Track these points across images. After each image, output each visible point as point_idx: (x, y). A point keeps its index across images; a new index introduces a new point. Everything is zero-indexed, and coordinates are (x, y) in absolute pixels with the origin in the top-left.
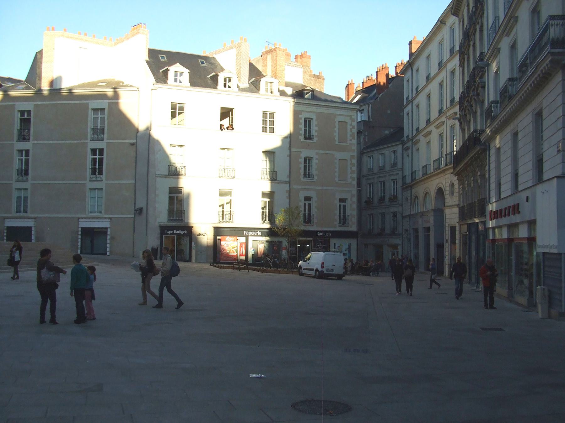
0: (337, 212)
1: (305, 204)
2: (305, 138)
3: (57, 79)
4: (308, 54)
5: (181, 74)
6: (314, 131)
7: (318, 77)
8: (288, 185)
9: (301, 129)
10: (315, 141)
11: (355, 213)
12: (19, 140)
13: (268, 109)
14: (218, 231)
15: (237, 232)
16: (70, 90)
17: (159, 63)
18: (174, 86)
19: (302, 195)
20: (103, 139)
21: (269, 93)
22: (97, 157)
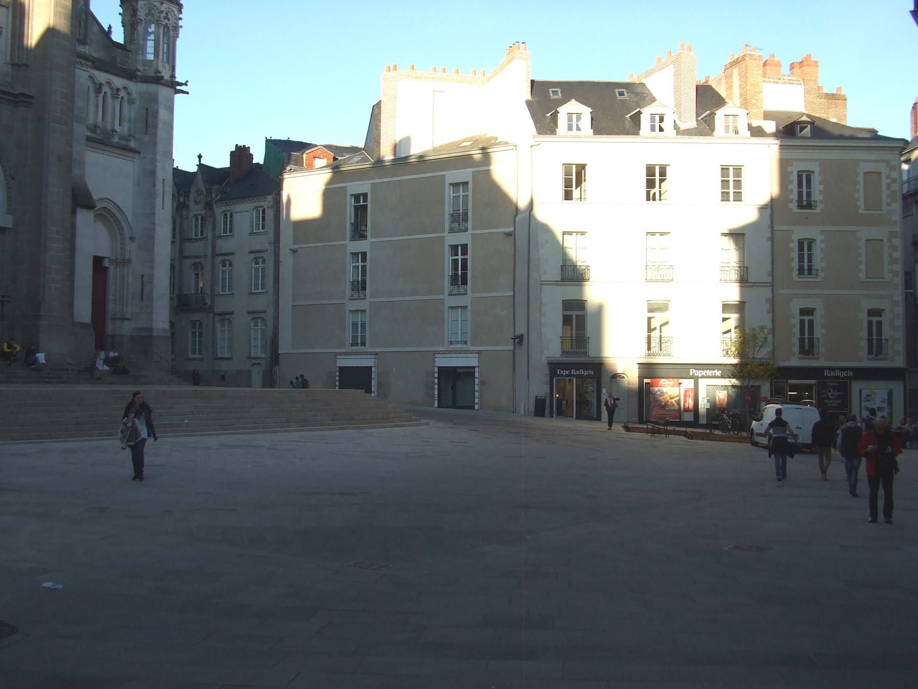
0: (864, 334)
1: (802, 322)
2: (801, 206)
3: (401, 141)
4: (813, 59)
5: (579, 116)
6: (817, 193)
7: (836, 98)
8: (769, 290)
9: (791, 191)
10: (818, 210)
11: (900, 334)
12: (353, 239)
13: (657, 160)
14: (649, 370)
15: (681, 371)
16: (421, 157)
17: (545, 101)
18: (567, 137)
19: (796, 305)
20: (466, 230)
21: (731, 134)
22: (460, 257)
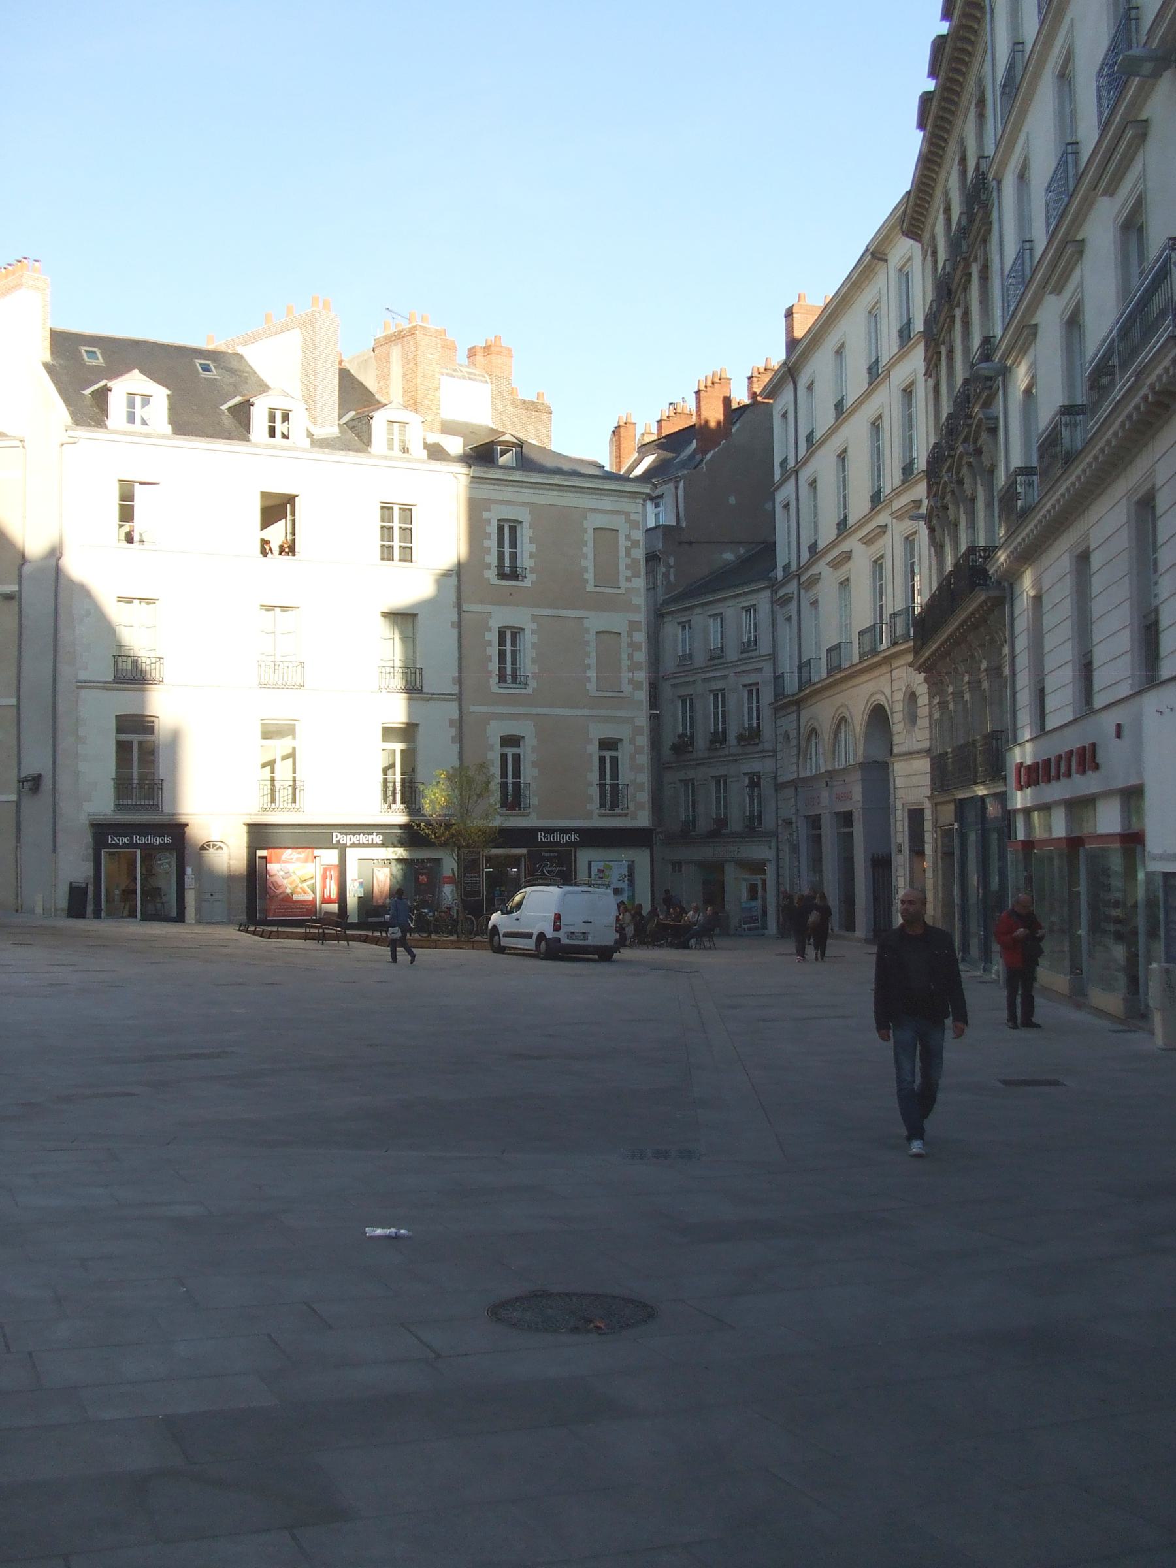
0: (594, 777)
2: (502, 575)
5: (146, 400)
7: (536, 408)
8: (455, 705)
9: (488, 551)
10: (527, 583)
11: (644, 778)
13: (397, 497)
14: (261, 836)
15: (314, 836)
18: (124, 433)
19: (495, 731)
21: (396, 451)
